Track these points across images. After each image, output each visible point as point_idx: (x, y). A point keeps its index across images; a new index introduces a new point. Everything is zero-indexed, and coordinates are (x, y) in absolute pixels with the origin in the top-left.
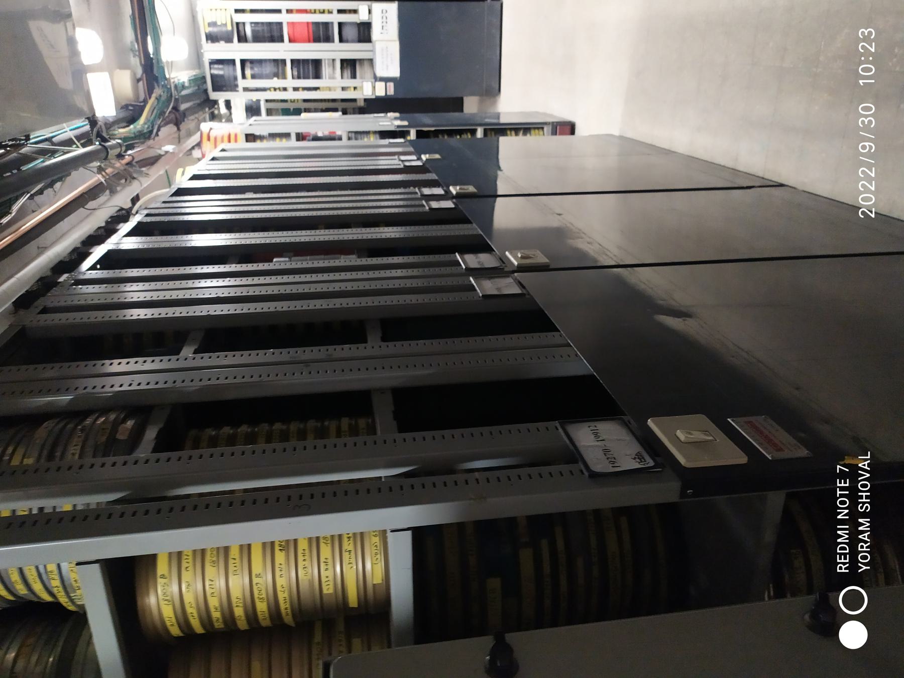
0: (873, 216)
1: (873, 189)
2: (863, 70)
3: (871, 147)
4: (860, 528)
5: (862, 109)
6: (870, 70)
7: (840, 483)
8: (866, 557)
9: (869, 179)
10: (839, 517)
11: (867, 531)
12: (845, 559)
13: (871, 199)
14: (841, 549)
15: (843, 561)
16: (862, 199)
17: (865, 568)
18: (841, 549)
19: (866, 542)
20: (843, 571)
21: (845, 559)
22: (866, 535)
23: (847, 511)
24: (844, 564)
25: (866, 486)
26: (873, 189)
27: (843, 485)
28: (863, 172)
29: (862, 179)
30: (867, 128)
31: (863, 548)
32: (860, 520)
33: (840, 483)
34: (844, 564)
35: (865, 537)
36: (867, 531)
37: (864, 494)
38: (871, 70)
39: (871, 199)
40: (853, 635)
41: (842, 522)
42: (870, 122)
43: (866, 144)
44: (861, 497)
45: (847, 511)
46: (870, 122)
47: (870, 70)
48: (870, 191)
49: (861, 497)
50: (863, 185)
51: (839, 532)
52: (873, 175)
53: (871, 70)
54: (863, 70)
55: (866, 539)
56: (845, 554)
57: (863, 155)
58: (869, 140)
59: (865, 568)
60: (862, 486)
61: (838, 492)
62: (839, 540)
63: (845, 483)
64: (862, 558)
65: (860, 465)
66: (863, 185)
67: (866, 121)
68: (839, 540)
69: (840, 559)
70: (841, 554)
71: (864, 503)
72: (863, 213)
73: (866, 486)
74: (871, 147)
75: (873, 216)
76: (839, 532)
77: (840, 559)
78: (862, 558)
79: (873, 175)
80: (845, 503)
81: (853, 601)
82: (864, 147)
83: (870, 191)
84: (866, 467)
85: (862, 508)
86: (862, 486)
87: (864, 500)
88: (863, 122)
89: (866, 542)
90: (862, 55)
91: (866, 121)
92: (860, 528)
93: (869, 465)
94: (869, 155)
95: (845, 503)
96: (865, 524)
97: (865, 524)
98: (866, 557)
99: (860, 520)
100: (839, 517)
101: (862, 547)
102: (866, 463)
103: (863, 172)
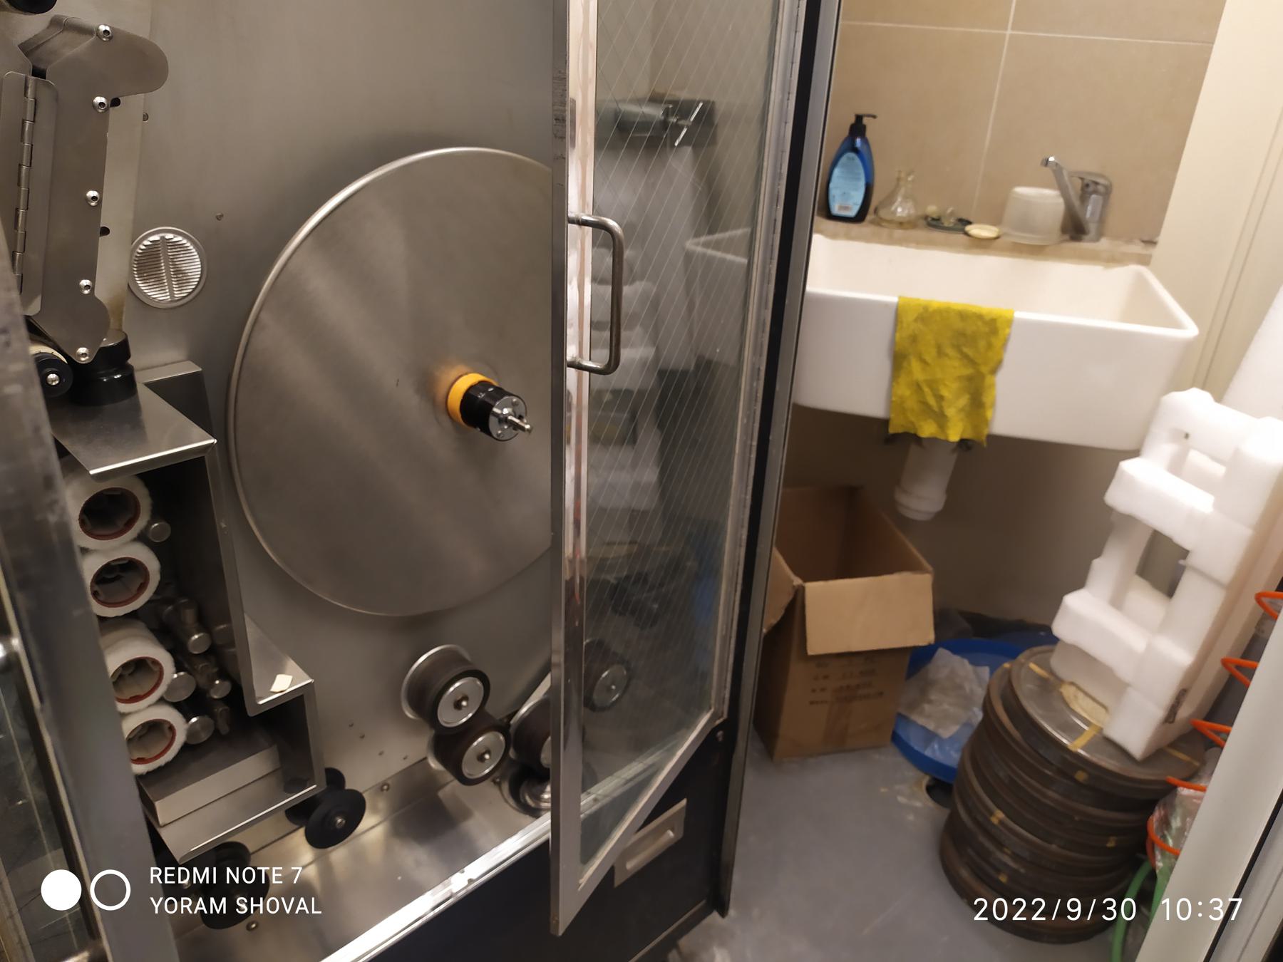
0: (977, 918)
1: (1015, 918)
2: (1184, 904)
3: (1074, 915)
4: (212, 900)
5: (1000, 903)
6: (1184, 914)
7: (277, 872)
8: (171, 908)
9: (1031, 910)
10: (229, 870)
11: (208, 909)
12: (169, 879)
13: (1000, 914)
14: (184, 873)
15: (167, 875)
16: (1000, 903)
17: (157, 906)
18: (184, 873)
19: (193, 908)
20: (152, 876)
21: (169, 879)
22: (204, 908)
23: (237, 881)
24: (162, 877)
25: (273, 908)
26: (1015, 918)
27: (274, 875)
28: (1039, 904)
29: (1029, 902)
30: (1101, 909)
31: (186, 905)
32: (224, 900)
33: (277, 872)
34: (162, 877)
35: (200, 905)
36: (208, 909)
37: (261, 905)
38: (1184, 915)
39: (1000, 914)
40: (61, 890)
41: (222, 874)
42: (1110, 914)
43: (1079, 909)
44: (257, 902)
45: (237, 881)
46: (1110, 914)
47: (1184, 914)
48: (1011, 915)
49: (257, 902)
50: (1020, 904)
51: (207, 870)
52: (1034, 918)
53: (1184, 915)
54: (1184, 904)
55: (198, 908)
56: (175, 878)
57: (1063, 905)
58: (1085, 912)
59: (157, 906)
60: (273, 903)
61: (263, 869)
62: (195, 870)
63: (277, 879)
64: (171, 903)
65: (302, 900)
66: (1020, 904)
67: (1111, 908)
68: (195, 870)
69: (169, 872)
70: (175, 872)
71: (248, 905)
72: (981, 904)
73: (273, 908)
74: (1074, 915)
75: (977, 918)
76: (207, 870)
77: (169, 872)
78: (171, 903)
79: (1034, 918)
80: (249, 878)
81: (110, 890)
82: (1074, 905)
83: (1011, 915)
84: (299, 908)
85: (242, 902)
86: (273, 903)
87: (252, 905)
88: (1110, 904)
89: (193, 908)
90: (1206, 902)
91: (1111, 908)
92: (212, 900)
93: (302, 912)
94: (1063, 912)
95: (249, 878)
96: (219, 906)
97: (219, 906)
98: (171, 908)
99: (224, 900)
100: (229, 870)
101: (186, 902)
102: (305, 908)
103: (1039, 904)
